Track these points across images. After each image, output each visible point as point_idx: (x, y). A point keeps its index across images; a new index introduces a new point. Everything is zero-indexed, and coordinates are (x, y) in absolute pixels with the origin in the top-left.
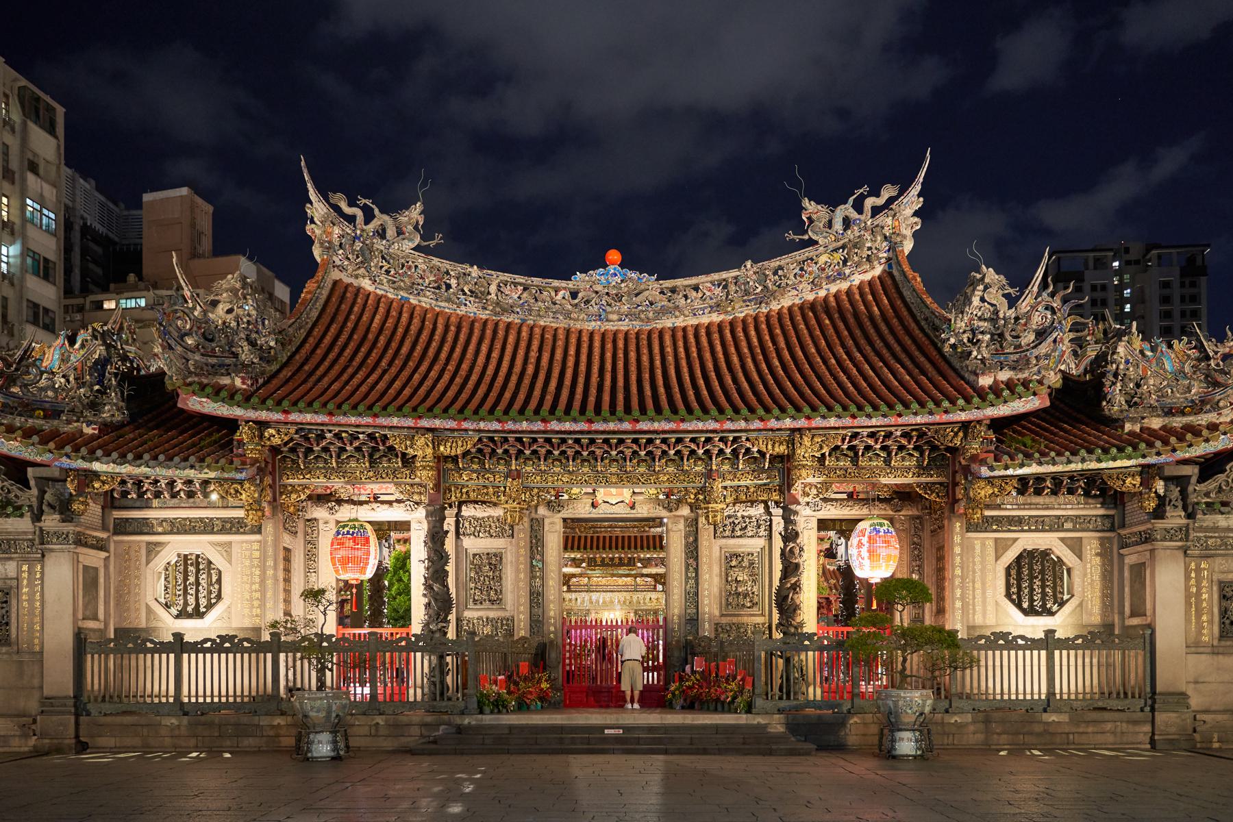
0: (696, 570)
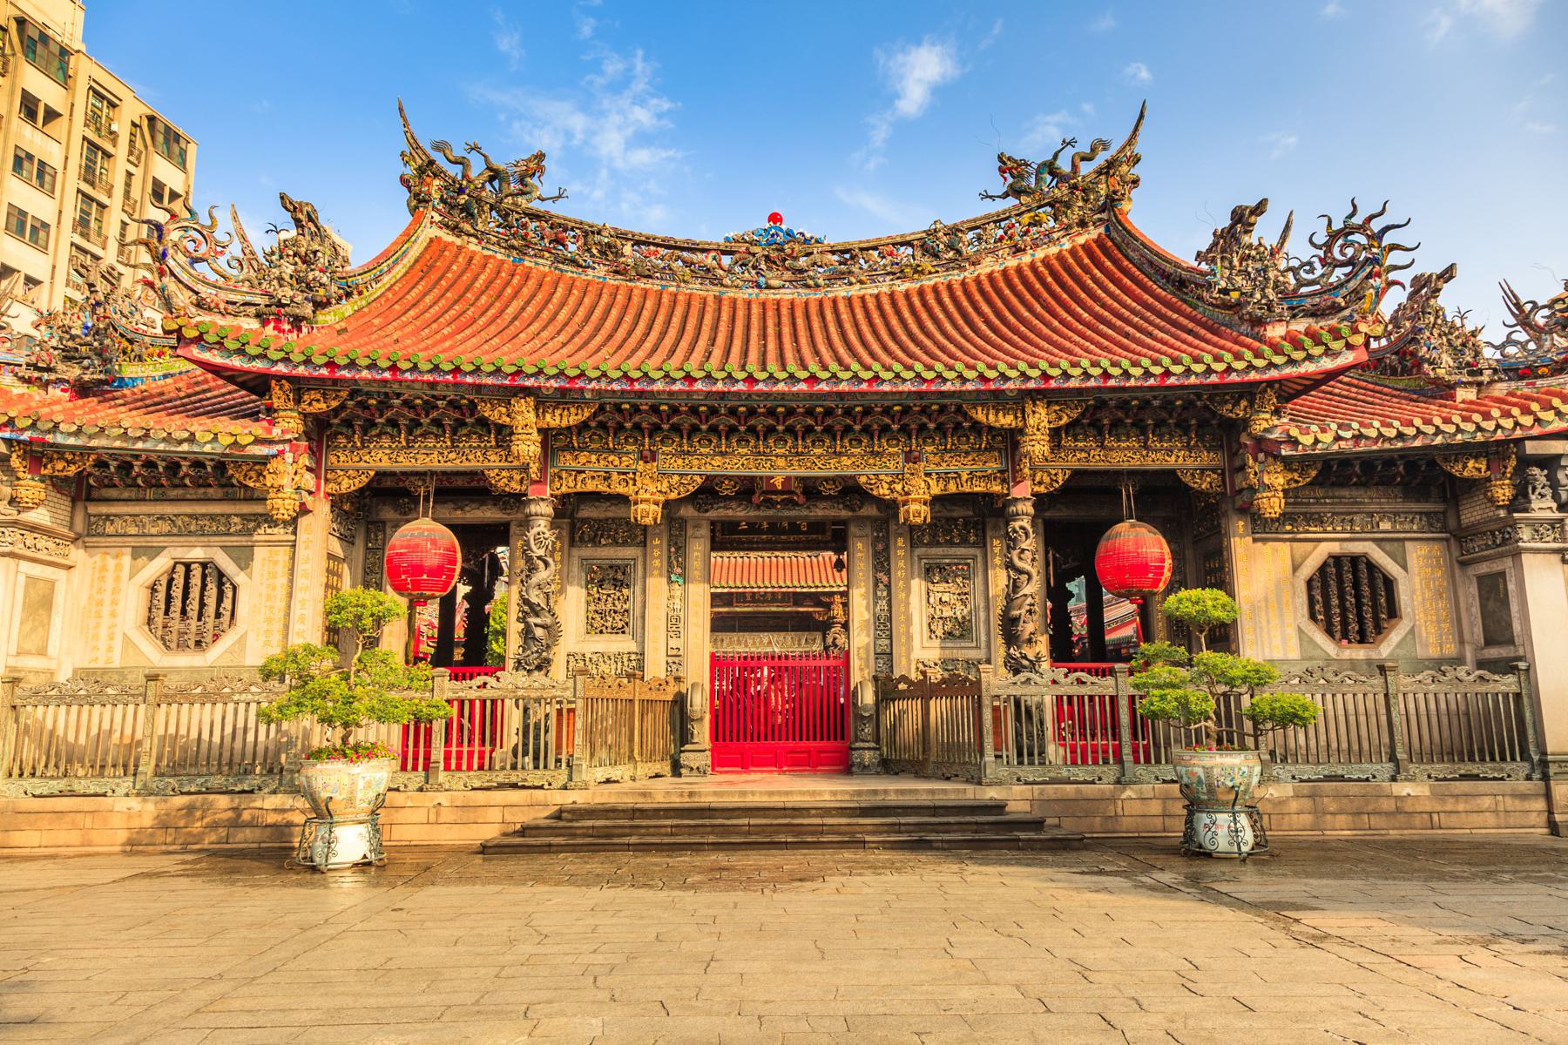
0: (888, 587)
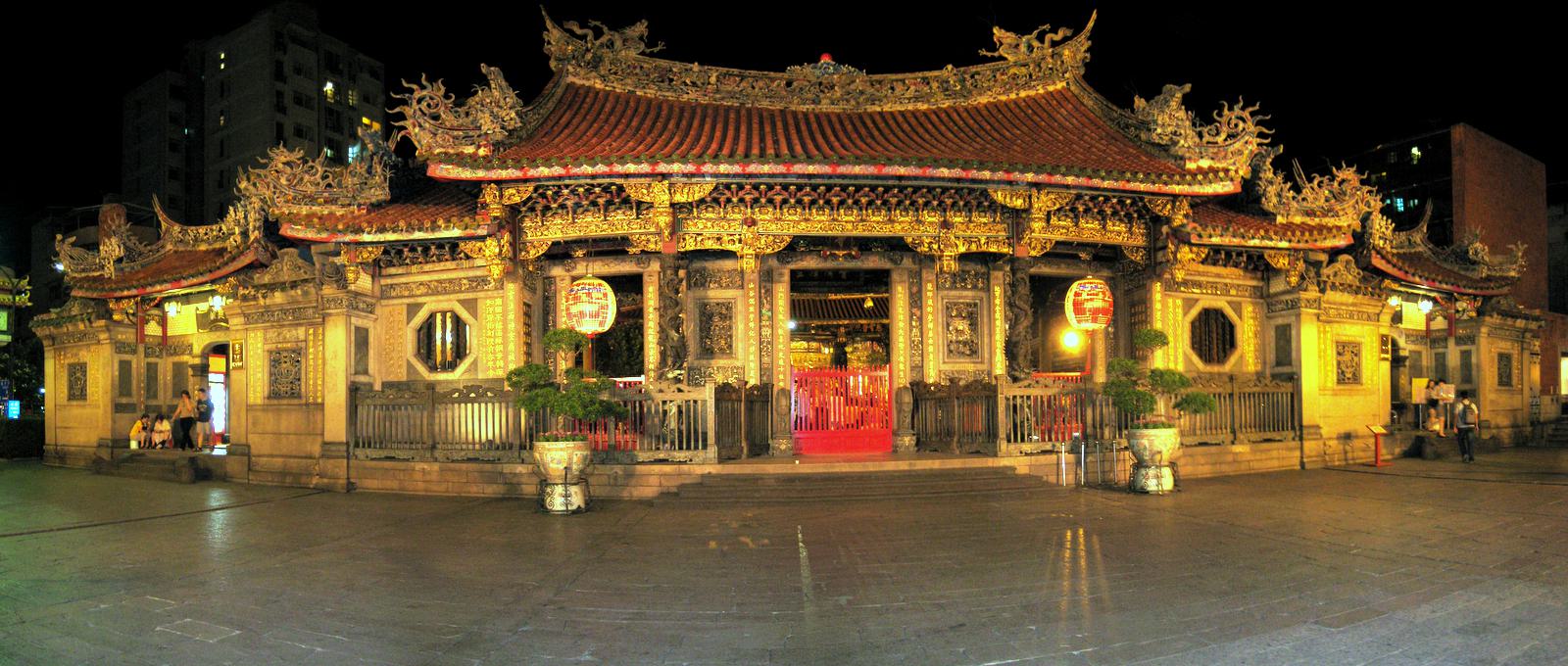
0: (920, 319)
